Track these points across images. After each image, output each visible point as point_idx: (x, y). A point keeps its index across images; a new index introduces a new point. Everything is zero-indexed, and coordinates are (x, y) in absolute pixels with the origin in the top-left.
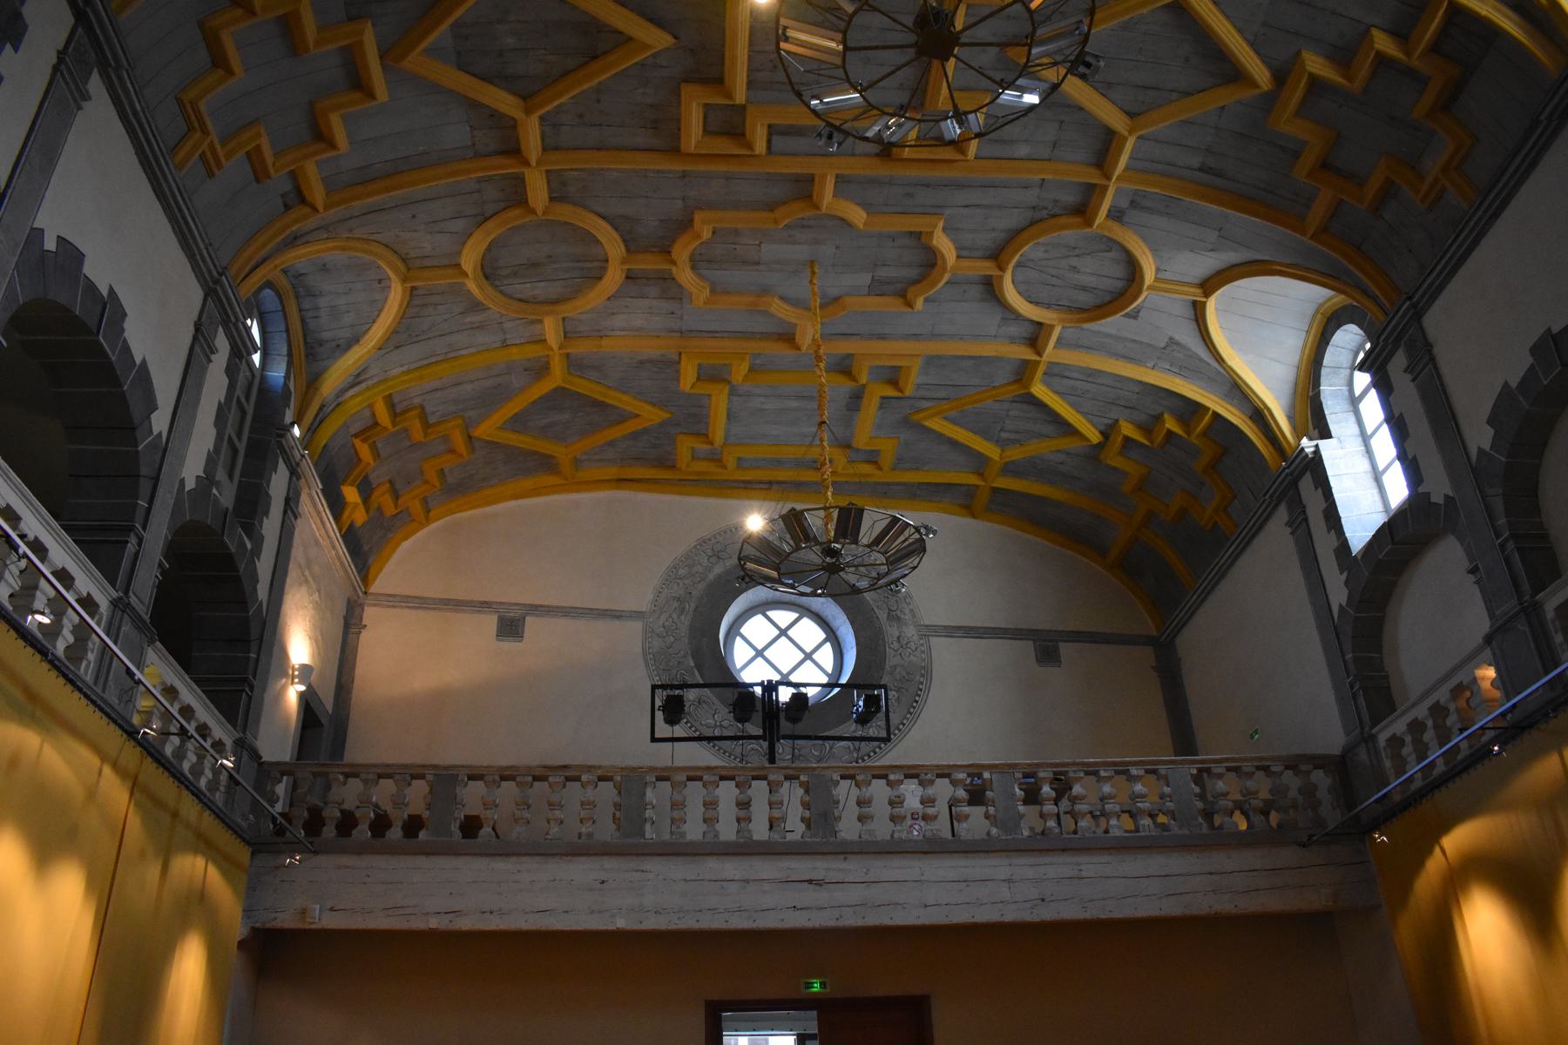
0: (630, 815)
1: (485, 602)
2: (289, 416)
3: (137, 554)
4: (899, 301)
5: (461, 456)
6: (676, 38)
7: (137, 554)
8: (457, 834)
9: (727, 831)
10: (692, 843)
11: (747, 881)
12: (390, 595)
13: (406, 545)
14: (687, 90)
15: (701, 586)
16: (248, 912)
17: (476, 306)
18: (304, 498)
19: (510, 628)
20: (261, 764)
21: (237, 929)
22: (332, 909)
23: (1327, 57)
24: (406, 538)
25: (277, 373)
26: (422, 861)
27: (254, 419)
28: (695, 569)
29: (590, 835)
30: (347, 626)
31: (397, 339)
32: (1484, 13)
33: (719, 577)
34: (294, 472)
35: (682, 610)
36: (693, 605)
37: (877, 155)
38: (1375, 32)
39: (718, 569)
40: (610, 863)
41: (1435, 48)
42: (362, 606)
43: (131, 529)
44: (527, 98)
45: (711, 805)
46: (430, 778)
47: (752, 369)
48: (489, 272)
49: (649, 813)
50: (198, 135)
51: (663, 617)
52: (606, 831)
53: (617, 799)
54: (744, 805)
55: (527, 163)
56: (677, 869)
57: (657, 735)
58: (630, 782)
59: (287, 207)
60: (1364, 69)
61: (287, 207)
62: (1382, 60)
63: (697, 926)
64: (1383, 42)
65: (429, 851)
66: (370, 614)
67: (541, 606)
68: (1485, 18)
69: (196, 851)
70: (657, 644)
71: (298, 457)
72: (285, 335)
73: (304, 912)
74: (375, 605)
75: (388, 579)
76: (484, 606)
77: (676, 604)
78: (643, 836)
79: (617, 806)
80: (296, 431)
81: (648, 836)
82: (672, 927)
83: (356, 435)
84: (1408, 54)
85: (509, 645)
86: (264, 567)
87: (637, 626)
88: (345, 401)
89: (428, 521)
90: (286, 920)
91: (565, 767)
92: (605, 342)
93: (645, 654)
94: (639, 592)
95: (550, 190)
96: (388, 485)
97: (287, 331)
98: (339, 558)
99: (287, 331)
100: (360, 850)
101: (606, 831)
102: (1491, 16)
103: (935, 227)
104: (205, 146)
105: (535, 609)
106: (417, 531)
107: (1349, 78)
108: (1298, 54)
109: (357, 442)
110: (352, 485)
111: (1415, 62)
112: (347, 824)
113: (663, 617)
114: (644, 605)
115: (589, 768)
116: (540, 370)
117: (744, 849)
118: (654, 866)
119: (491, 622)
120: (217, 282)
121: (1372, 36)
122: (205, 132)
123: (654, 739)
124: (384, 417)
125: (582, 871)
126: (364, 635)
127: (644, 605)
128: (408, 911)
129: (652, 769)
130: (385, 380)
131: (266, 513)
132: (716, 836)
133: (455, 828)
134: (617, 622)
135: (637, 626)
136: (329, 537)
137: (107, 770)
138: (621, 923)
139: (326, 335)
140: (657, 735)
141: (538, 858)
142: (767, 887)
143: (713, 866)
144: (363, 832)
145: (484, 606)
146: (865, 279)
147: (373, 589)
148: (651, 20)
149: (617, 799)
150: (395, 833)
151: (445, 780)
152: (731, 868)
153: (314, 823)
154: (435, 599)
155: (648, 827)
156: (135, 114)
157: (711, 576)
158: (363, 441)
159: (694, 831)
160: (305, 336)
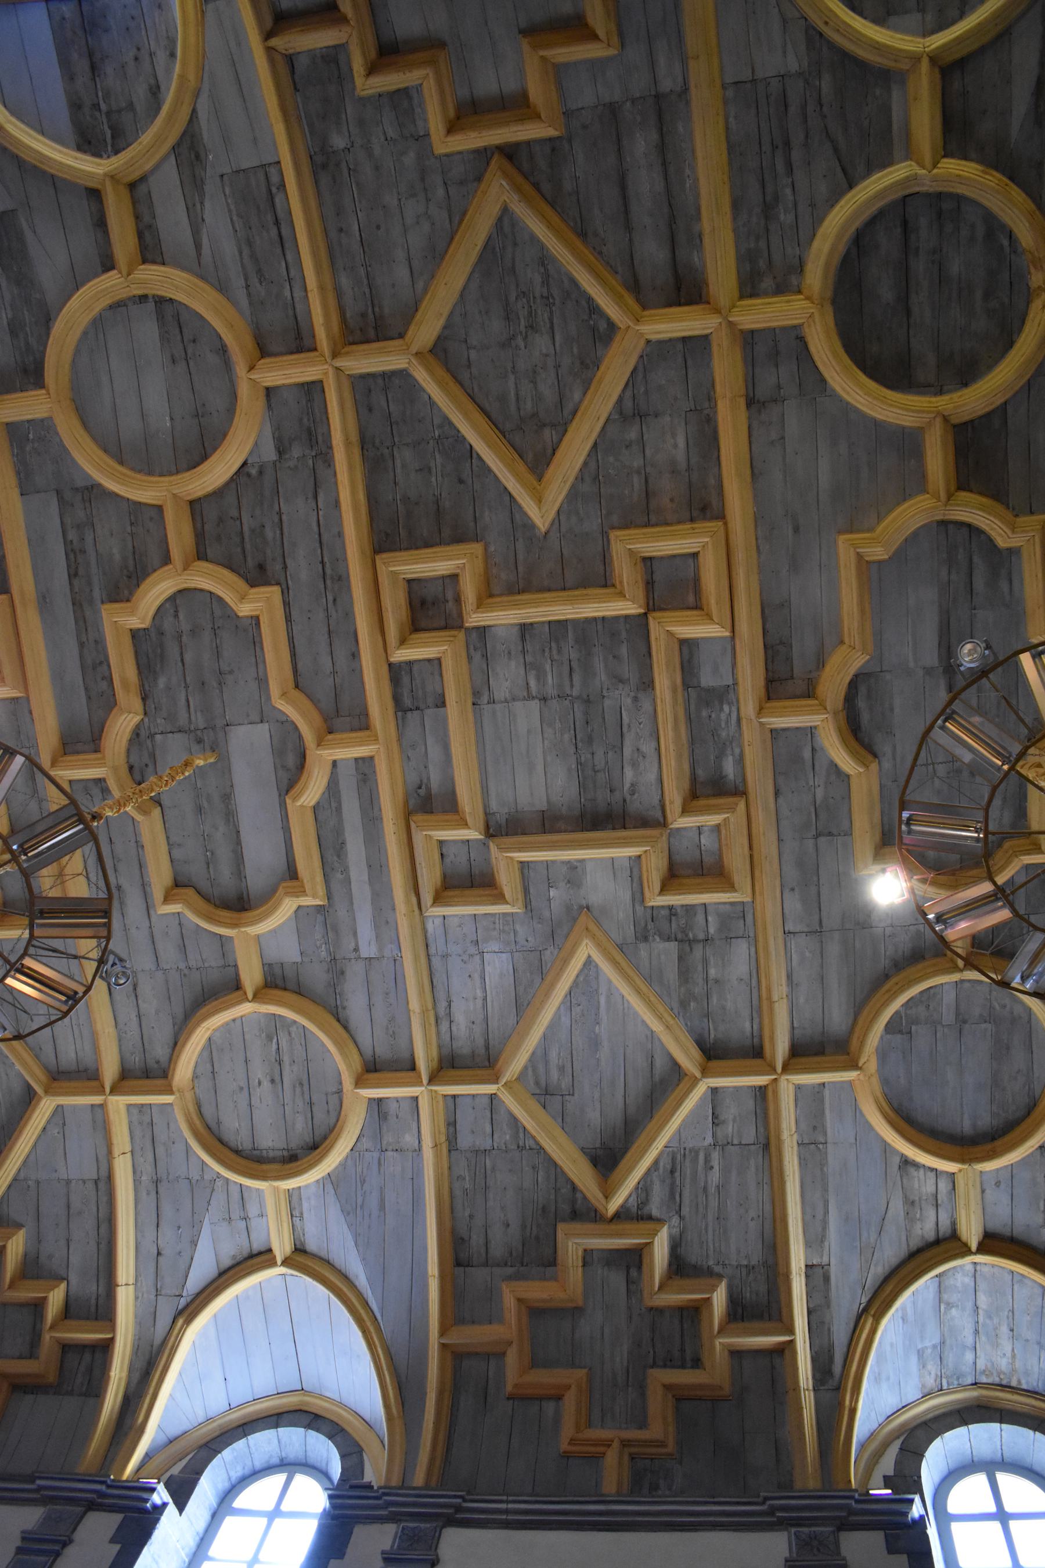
23: (25, 1255)
32: (112, 1374)
38: (63, 1286)
41: (66, 1348)
60: (27, 1293)
62: (38, 1306)
64: (56, 1298)
68: (109, 1377)
84: (53, 1327)
102: (111, 1382)
107: (11, 1286)
108: (19, 1226)
111: (47, 1337)
121: (57, 1286)
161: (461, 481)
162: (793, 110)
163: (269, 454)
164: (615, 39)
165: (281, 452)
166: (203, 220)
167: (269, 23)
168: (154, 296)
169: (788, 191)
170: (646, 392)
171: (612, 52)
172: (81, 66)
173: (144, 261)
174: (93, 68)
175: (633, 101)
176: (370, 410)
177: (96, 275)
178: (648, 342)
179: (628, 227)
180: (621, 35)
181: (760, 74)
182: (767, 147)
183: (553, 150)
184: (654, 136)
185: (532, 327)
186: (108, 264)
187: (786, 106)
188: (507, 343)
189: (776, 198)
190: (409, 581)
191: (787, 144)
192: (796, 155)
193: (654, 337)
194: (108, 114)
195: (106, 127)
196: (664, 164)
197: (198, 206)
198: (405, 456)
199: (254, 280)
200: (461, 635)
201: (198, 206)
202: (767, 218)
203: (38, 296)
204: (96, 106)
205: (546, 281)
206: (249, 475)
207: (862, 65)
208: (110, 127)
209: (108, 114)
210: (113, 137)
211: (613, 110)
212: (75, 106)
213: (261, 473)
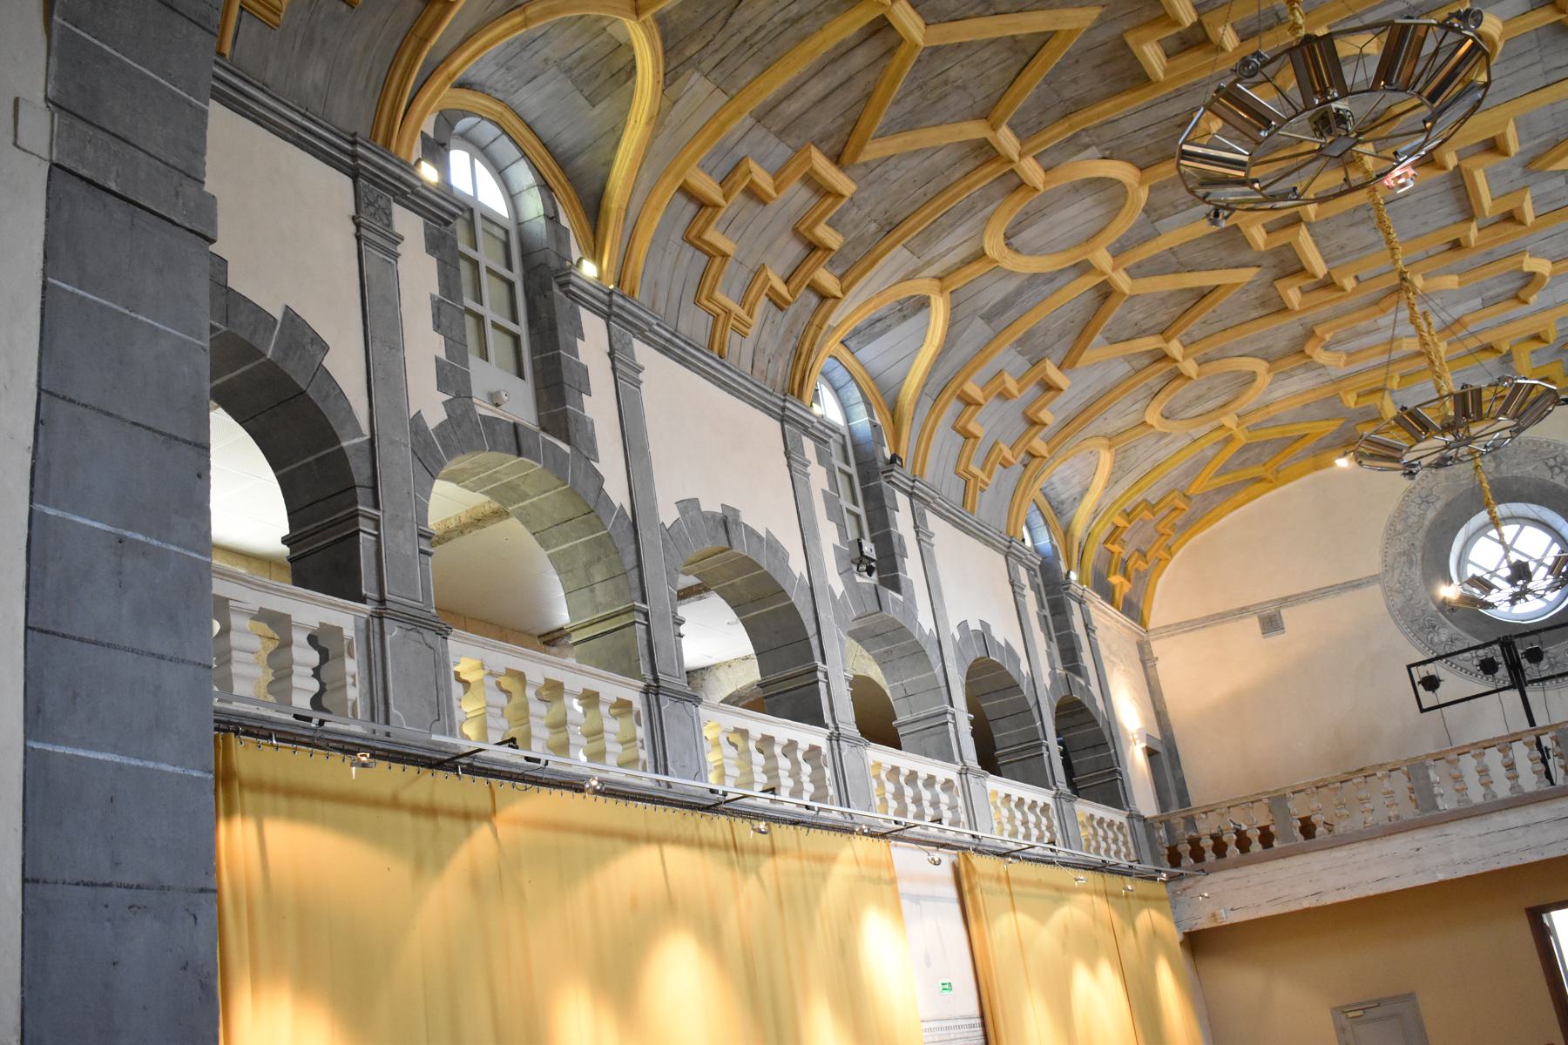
0: (1423, 794)
1: (1243, 608)
2: (1064, 569)
3: (1049, 756)
4: (1514, 302)
5: (1184, 510)
6: (1259, 266)
7: (1049, 756)
8: (1301, 837)
9: (1502, 789)
10: (1477, 807)
11: (1528, 826)
12: (1166, 627)
13: (1161, 580)
14: (1279, 284)
15: (1421, 535)
16: (1177, 923)
17: (1164, 435)
18: (1091, 609)
19: (1271, 624)
20: (1145, 820)
21: (1176, 937)
22: (1232, 910)
24: (1160, 575)
25: (1044, 541)
26: (1281, 863)
27: (1045, 586)
28: (1410, 521)
29: (1397, 817)
30: (1143, 662)
31: (1113, 480)
33: (1434, 523)
34: (1080, 603)
35: (1411, 563)
36: (1419, 555)
37: (1450, 249)
39: (1431, 515)
40: (1420, 835)
42: (1148, 643)
43: (1041, 745)
44: (1164, 332)
45: (1483, 771)
46: (1266, 801)
47: (1402, 377)
48: (1166, 416)
49: (1436, 790)
50: (972, 481)
51: (1397, 572)
52: (1409, 812)
53: (1409, 785)
54: (1510, 766)
55: (1176, 361)
56: (1472, 828)
57: (1424, 707)
58: (1416, 770)
59: (1026, 466)
61: (1026, 466)
63: (1498, 867)
65: (1285, 854)
66: (1157, 647)
67: (1289, 597)
69: (1141, 908)
70: (1399, 600)
71: (1080, 592)
72: (1038, 512)
73: (1214, 915)
74: (1157, 639)
76: (1243, 612)
77: (1404, 559)
78: (1436, 807)
79: (1412, 790)
80: (1073, 576)
81: (1441, 808)
82: (1481, 871)
83: (1105, 542)
85: (1276, 639)
86: (1095, 689)
87: (1376, 590)
88: (1093, 530)
89: (1172, 555)
90: (1204, 923)
91: (1362, 770)
93: (1390, 612)
94: (1370, 561)
96: (1136, 554)
97: (1039, 508)
98: (1123, 625)
99: (1039, 508)
100: (1236, 865)
101: (1409, 812)
103: (1523, 200)
104: (980, 484)
105: (1286, 601)
106: (1166, 566)
109: (1109, 546)
110: (1115, 574)
112: (1220, 848)
113: (1397, 572)
114: (1376, 568)
115: (1381, 766)
116: (1229, 440)
117: (1521, 801)
118: (1453, 829)
119: (1253, 623)
122: (975, 477)
123: (1422, 711)
124: (1121, 522)
125: (1400, 844)
126: (1160, 666)
127: (1376, 568)
128: (1286, 899)
129: (1428, 756)
130: (1114, 503)
131: (1081, 650)
132: (1494, 796)
133: (1297, 833)
134: (1357, 592)
135: (1376, 590)
136: (1113, 618)
137: (1095, 898)
138: (1441, 877)
139: (1064, 497)
140: (1424, 707)
141: (1365, 843)
142: (1545, 827)
143: (1498, 820)
144: (1233, 851)
145: (1243, 612)
146: (1477, 302)
147: (1150, 627)
148: (1236, 267)
149: (1409, 785)
150: (1256, 847)
151: (1278, 802)
152: (1514, 818)
153: (1197, 854)
154: (1201, 618)
155: (1439, 801)
156: (947, 510)
157: (1427, 523)
158: (1112, 544)
159: (1476, 795)
160: (1050, 503)
161: (1077, 61)
162: (720, 55)
163: (1093, 150)
164: (743, 169)
165: (1088, 146)
167: (830, 302)
169: (775, 19)
170: (965, 5)
171: (753, 165)
173: (985, 254)
175: (769, 129)
176: (1041, 123)
178: (927, 24)
179: (850, 78)
180: (737, 166)
181: (713, 87)
182: (755, 49)
183: (821, 142)
184: (784, 105)
185: (946, 83)
187: (722, 60)
188: (964, 88)
189: (785, 21)
190: (1168, 56)
191: (745, 41)
192: (748, 32)
193: (921, 23)
196: (798, 89)
198: (1068, 93)
199: (977, 209)
200: (1206, 19)
202: (802, 17)
204: (900, 310)
205: (911, 93)
206: (1111, 154)
207: (664, 40)
211: (780, 134)
213: (1107, 149)
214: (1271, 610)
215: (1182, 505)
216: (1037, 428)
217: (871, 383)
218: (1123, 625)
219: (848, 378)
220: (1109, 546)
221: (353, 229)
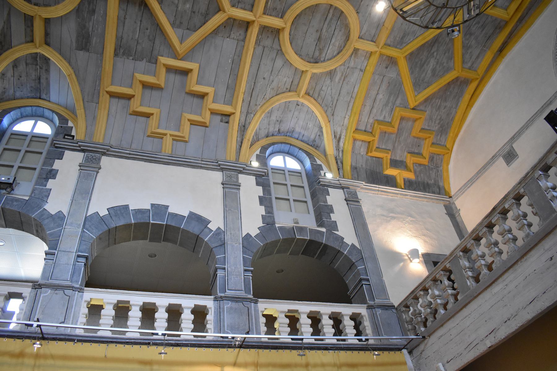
1: (493, 157)
5: (420, 118)
12: (459, 190)
22: (448, 362)
24: (448, 164)
67: (515, 135)
72: (300, 151)
74: (457, 199)
75: (454, 183)
76: (494, 158)
83: (367, 153)
85: (516, 164)
88: (343, 148)
92: (386, 25)
95: (277, 16)
97: (300, 149)
99: (300, 149)
105: (514, 139)
109: (370, 154)
110: (387, 169)
119: (501, 161)
120: (219, 165)
126: (462, 213)
128: (475, 343)
136: (398, 194)
139: (312, 137)
147: (452, 193)
154: (475, 175)
156: (130, 154)
158: (371, 152)
166: (4, 22)
168: (31, 4)
172: (43, 81)
174: (39, 79)
177: (53, 18)
186: (47, 21)
194: (37, 65)
195: (39, 61)
197: (5, 28)
201: (5, 28)
203: (78, 19)
204: (41, 68)
208: (37, 61)
209: (37, 65)
210: (37, 58)
212: (48, 71)
214: (507, 148)
215: (418, 116)
216: (206, 98)
217: (66, 111)
218: (411, 196)
219: (51, 112)
220: (370, 154)
221: (345, 202)
